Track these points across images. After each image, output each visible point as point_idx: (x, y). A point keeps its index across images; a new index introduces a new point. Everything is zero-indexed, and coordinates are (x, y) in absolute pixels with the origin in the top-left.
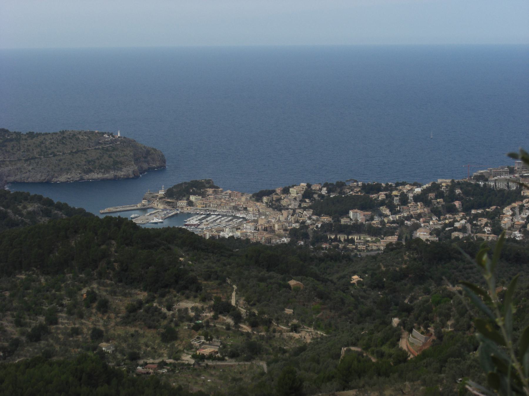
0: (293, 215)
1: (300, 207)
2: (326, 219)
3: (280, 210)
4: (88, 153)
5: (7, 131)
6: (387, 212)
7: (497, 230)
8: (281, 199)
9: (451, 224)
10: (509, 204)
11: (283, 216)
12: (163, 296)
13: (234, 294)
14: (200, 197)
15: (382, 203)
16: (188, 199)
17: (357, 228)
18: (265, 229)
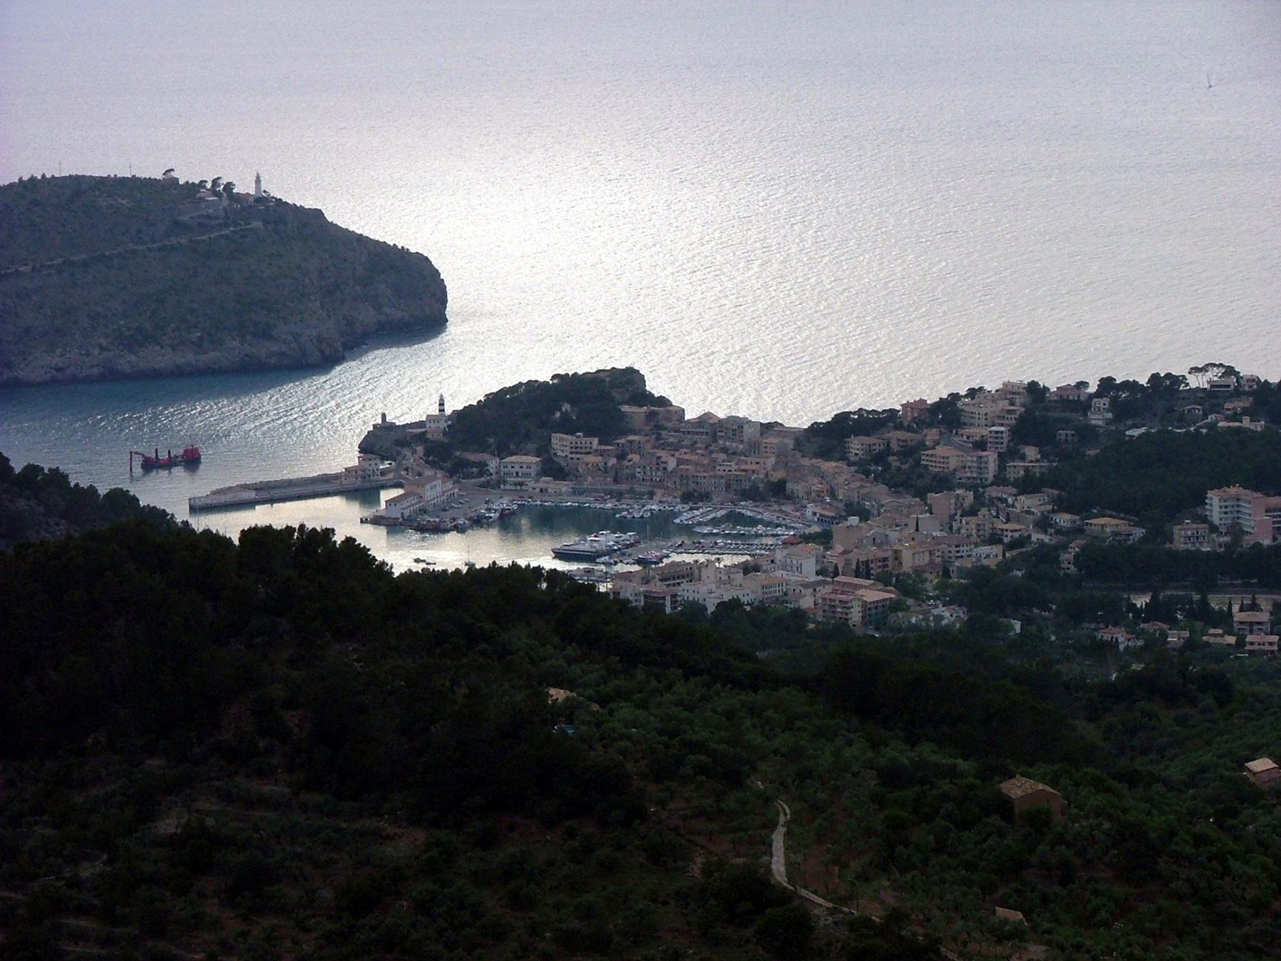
3: (921, 494)
8: (922, 445)
12: (488, 841)
13: (778, 840)
16: (544, 450)
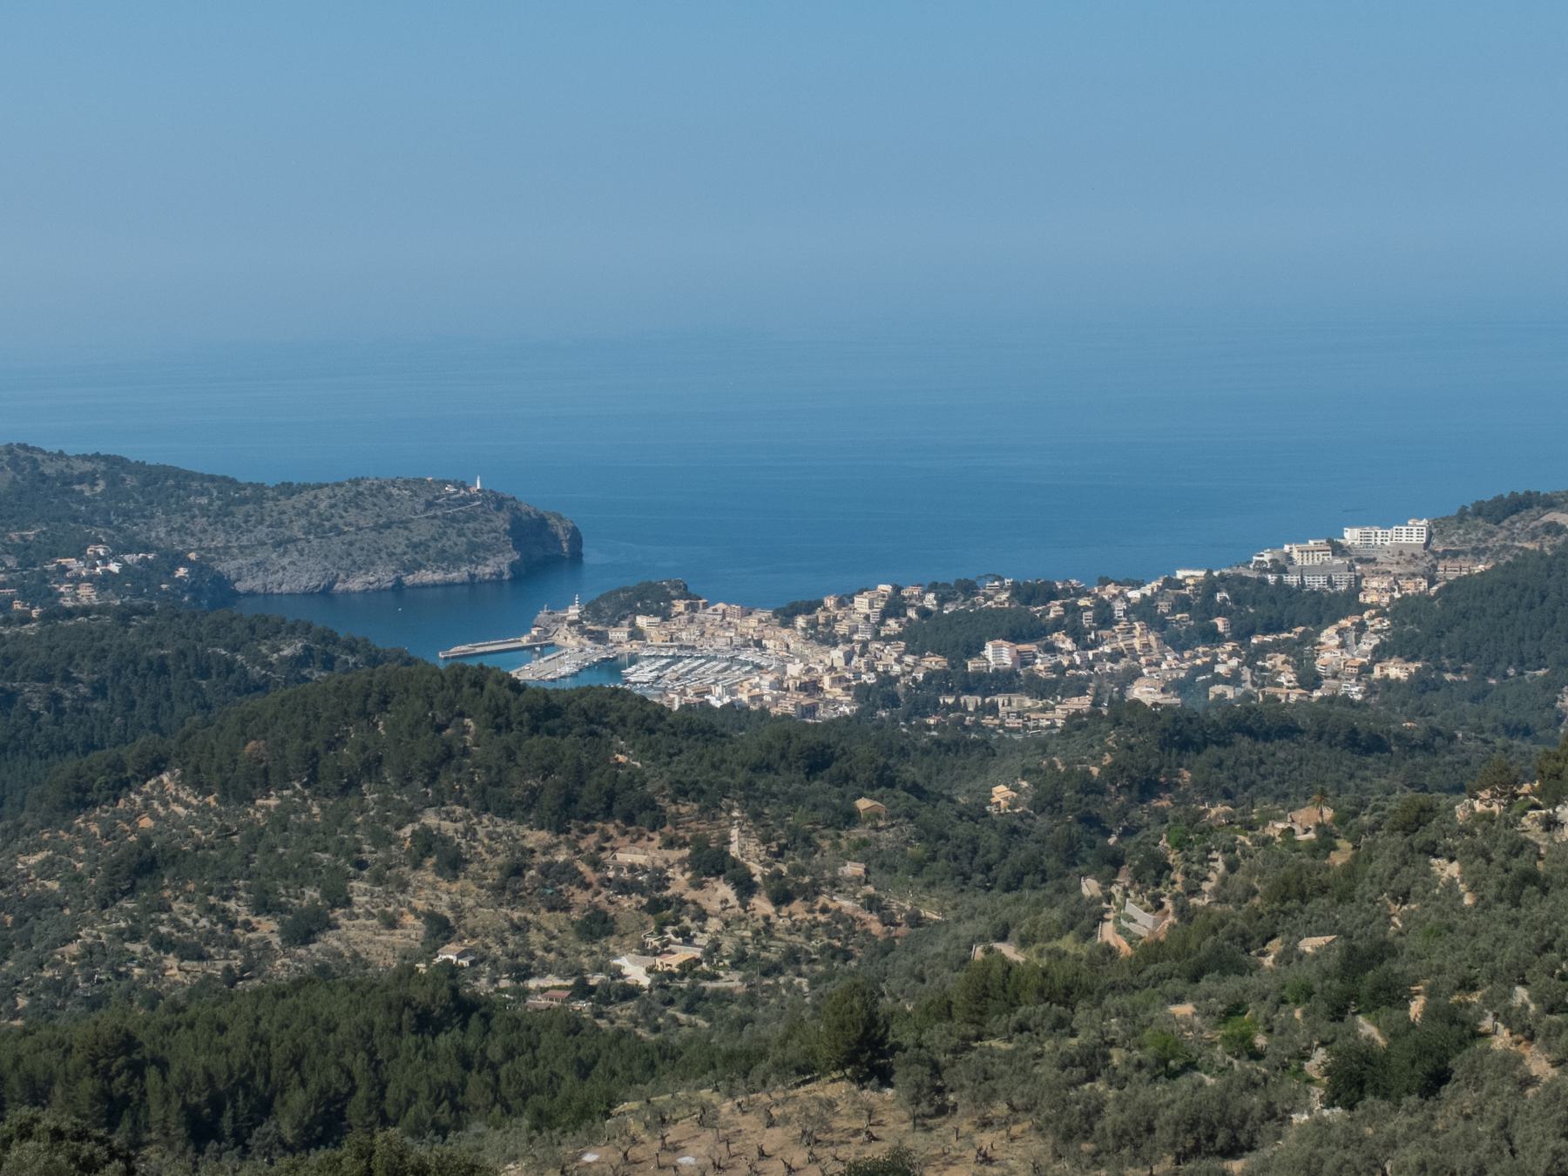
0: (861, 655)
1: (876, 636)
2: (934, 662)
4: (411, 526)
5: (233, 482)
6: (1068, 645)
7: (1309, 680)
8: (835, 620)
9: (1208, 668)
10: (1334, 621)
11: (837, 655)
14: (658, 619)
15: (1057, 625)
16: (633, 624)
17: (1005, 681)
18: (803, 688)
